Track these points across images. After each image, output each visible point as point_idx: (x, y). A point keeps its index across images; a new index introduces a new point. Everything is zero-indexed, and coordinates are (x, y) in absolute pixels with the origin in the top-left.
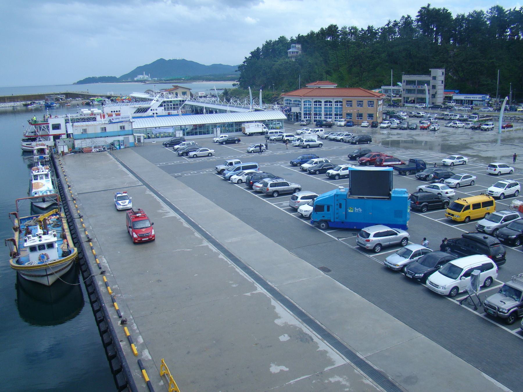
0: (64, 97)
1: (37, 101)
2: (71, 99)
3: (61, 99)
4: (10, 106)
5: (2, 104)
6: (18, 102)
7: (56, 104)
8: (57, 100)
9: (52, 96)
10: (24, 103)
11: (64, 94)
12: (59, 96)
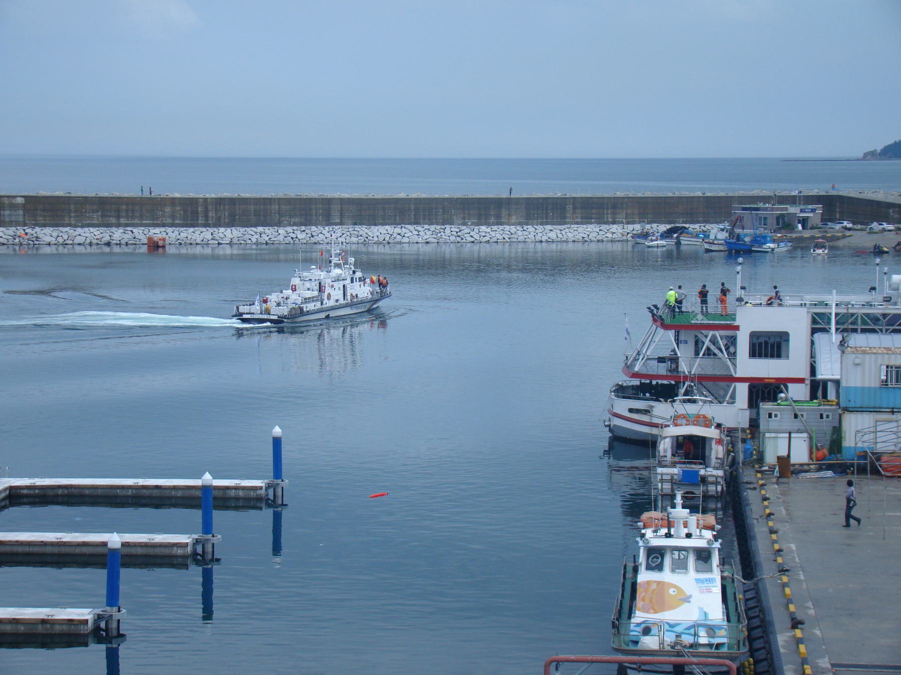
0: (815, 214)
1: (697, 226)
2: (845, 223)
3: (804, 222)
4: (579, 237)
5: (549, 227)
6: (614, 223)
7: (774, 241)
8: (785, 224)
9: (761, 205)
10: (637, 227)
11: (818, 199)
12: (793, 210)
